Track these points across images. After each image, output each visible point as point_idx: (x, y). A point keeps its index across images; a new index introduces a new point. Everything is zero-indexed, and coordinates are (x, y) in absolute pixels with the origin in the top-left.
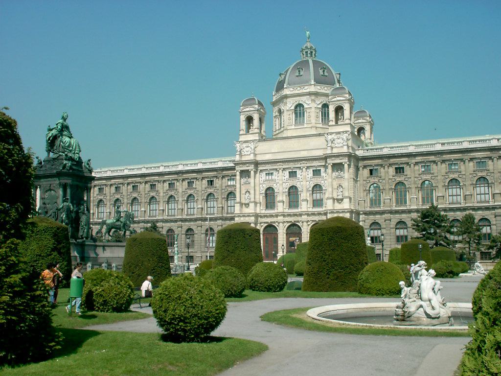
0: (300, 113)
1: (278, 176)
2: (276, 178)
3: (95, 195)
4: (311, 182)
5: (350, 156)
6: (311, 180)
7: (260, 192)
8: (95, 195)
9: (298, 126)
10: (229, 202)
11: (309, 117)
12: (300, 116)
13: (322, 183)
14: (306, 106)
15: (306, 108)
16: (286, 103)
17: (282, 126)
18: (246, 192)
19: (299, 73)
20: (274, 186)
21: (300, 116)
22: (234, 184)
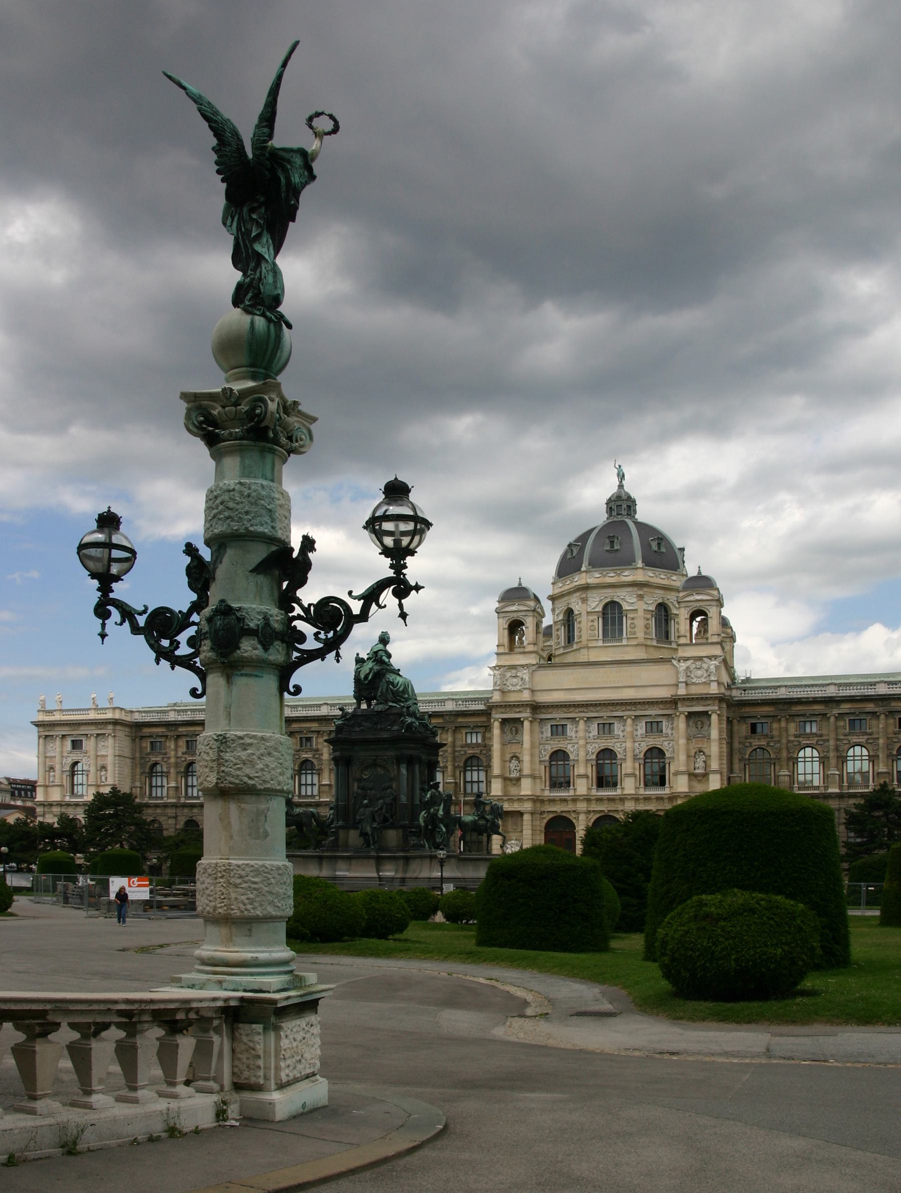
0: (613, 619)
1: (577, 732)
2: (573, 735)
3: (180, 754)
4: (643, 744)
5: (721, 699)
6: (643, 739)
7: (540, 758)
8: (180, 754)
9: (609, 641)
10: (468, 774)
11: (633, 626)
12: (613, 624)
13: (665, 746)
14: (625, 607)
15: (627, 610)
16: (584, 600)
17: (576, 640)
18: (512, 758)
19: (612, 546)
20: (569, 749)
21: (613, 624)
22: (480, 741)
